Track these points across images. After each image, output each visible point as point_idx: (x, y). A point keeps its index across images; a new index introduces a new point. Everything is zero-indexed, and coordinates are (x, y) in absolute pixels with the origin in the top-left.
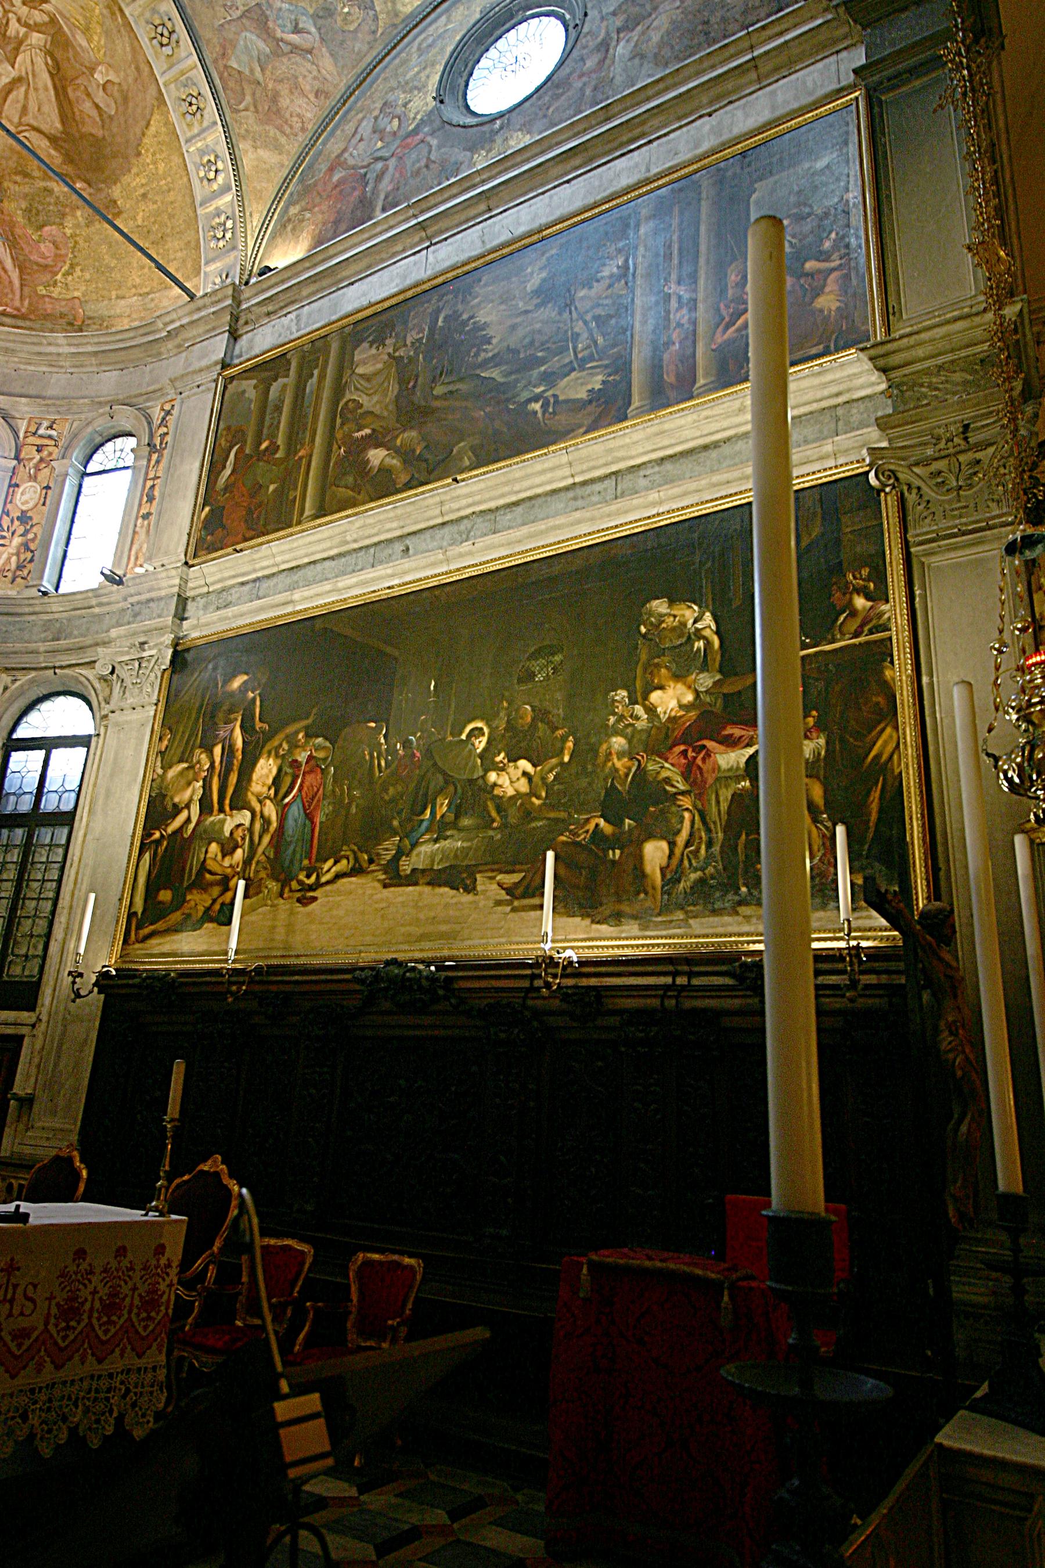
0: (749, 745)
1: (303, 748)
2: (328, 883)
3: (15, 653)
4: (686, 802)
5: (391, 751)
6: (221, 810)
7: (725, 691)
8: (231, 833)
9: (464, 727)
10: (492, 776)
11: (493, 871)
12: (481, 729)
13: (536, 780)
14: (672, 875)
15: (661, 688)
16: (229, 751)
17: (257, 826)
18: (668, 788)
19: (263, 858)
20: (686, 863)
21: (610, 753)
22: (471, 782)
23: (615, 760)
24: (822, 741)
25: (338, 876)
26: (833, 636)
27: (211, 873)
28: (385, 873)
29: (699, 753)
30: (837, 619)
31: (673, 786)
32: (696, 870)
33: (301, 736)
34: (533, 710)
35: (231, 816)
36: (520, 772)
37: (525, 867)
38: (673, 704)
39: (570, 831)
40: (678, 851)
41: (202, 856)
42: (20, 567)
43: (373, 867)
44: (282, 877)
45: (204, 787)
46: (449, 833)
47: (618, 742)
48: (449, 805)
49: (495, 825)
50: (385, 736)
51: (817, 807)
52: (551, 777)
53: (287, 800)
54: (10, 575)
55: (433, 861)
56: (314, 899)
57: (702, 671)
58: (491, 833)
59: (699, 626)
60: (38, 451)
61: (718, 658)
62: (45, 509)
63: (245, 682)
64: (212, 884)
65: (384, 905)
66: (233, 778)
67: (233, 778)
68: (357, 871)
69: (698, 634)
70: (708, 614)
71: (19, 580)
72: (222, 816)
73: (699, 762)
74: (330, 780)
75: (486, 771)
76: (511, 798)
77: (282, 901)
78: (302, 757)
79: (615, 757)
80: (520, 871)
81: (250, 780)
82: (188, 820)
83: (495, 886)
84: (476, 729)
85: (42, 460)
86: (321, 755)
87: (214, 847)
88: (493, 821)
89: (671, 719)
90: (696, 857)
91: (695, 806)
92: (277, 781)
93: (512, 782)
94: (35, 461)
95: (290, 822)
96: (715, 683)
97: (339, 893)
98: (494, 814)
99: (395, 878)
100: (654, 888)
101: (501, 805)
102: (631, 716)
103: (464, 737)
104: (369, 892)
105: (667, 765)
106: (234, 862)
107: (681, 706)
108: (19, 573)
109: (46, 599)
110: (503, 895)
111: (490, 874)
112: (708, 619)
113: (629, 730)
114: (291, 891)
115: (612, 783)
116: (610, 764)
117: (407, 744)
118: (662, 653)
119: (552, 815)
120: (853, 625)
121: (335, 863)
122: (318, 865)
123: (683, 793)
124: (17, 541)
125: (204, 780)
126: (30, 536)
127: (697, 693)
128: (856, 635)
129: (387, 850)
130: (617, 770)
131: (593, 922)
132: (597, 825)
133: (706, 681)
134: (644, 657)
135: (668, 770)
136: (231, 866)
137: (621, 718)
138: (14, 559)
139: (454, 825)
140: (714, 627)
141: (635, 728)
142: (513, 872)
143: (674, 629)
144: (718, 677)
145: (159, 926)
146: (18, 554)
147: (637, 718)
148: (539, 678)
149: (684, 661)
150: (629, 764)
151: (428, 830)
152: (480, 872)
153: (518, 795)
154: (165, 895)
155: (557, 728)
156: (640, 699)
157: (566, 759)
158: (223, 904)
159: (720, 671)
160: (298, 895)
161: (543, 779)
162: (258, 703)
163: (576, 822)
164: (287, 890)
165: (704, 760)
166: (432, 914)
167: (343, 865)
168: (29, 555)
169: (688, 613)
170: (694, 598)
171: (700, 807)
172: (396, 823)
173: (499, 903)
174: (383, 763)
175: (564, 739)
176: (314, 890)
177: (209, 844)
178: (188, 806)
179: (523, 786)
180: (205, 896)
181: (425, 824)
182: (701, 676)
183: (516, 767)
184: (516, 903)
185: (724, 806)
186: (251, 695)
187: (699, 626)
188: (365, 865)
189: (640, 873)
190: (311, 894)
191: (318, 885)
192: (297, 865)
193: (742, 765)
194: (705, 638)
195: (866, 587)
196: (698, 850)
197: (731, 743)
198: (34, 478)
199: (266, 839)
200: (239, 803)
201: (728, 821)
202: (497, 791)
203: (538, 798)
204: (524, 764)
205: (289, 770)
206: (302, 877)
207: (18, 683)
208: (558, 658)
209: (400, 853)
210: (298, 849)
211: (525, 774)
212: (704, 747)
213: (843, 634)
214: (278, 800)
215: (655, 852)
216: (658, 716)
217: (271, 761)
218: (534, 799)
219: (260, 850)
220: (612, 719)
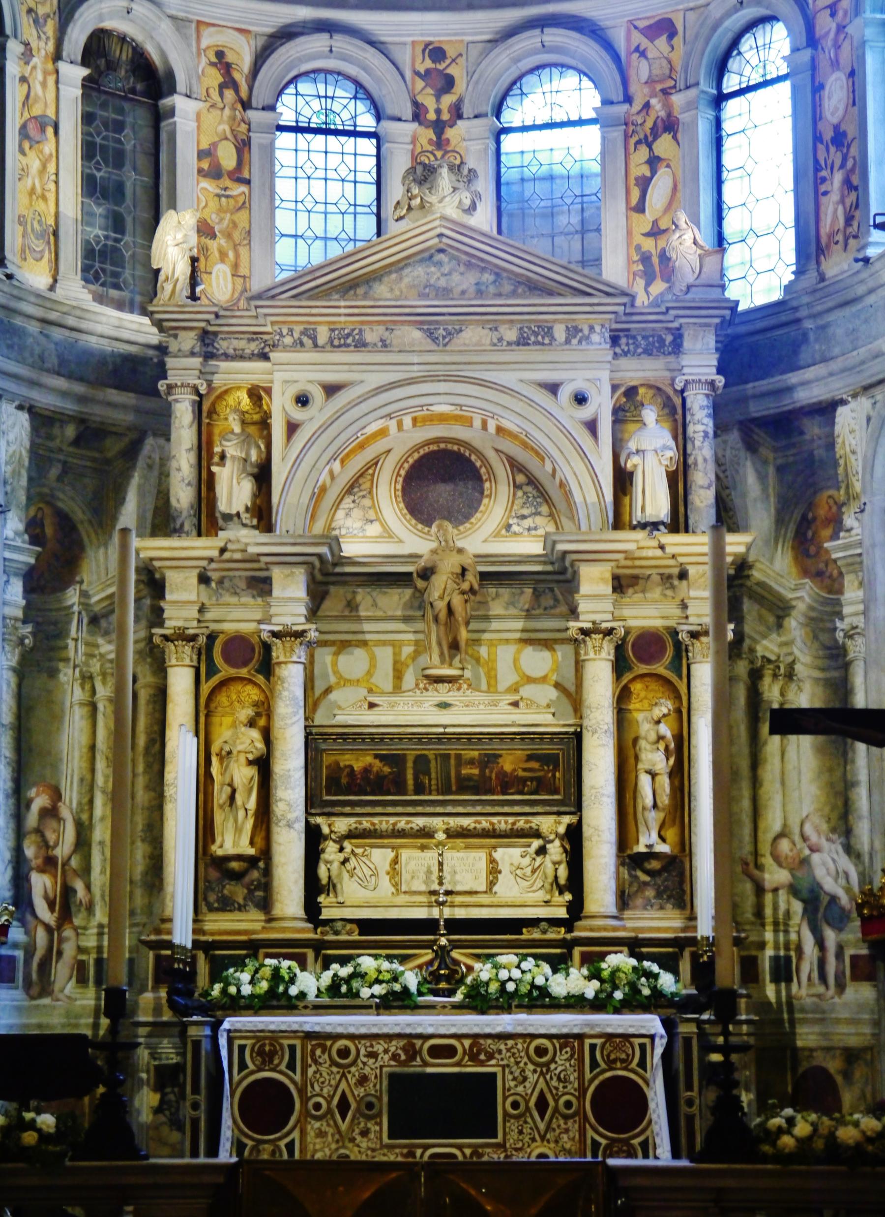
3: (863, 362)
42: (849, 220)
54: (840, 237)
60: (833, 15)
62: (856, 108)
71: (852, 242)
85: (841, 28)
94: (832, 35)
108: (850, 230)
109: (873, 269)
124: (838, 177)
126: (850, 164)
138: (840, 209)
146: (842, 201)
168: (853, 196)
198: (835, 64)
207: (878, 405)
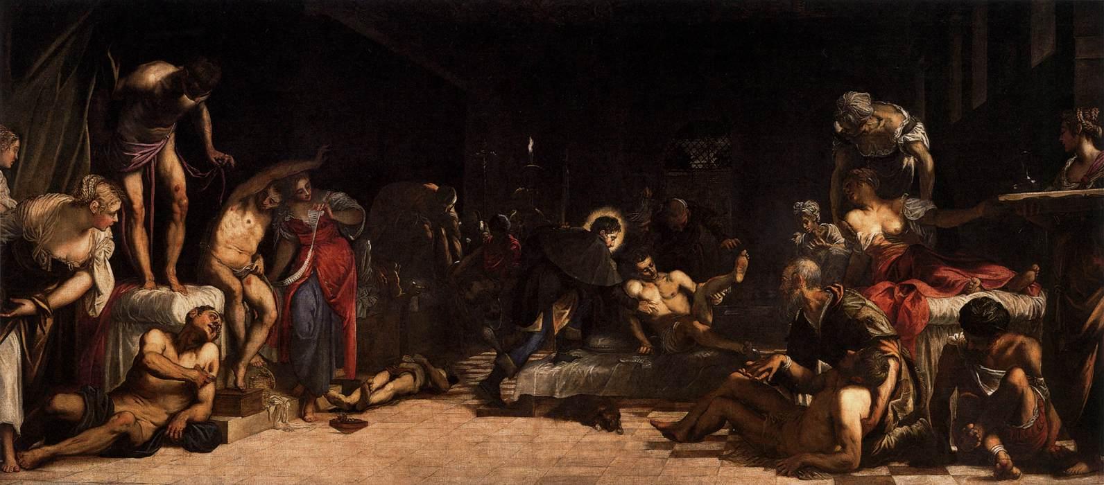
0: (965, 292)
1: (311, 203)
2: (382, 404)
4: (892, 348)
5: (469, 230)
6: (161, 280)
7: (939, 225)
8: (189, 318)
9: (588, 214)
10: (636, 287)
11: (644, 406)
12: (614, 221)
13: (699, 299)
14: (874, 429)
15: (863, 207)
16: (158, 187)
17: (240, 313)
18: (871, 330)
19: (258, 361)
20: (891, 415)
21: (798, 279)
22: (604, 291)
23: (805, 289)
24: (1042, 299)
25: (398, 397)
26: (1060, 182)
27: (156, 374)
28: (478, 397)
29: (908, 292)
30: (1064, 164)
31: (878, 329)
32: (901, 425)
33: (302, 184)
34: (689, 207)
35: (184, 292)
36: (674, 288)
37: (689, 405)
38: (876, 230)
39: (747, 367)
40: (882, 402)
41: (136, 349)
43: (455, 388)
44: (300, 389)
45: (117, 238)
46: (574, 354)
47: (809, 267)
48: (572, 318)
49: (643, 349)
50: (457, 207)
51: (1036, 370)
52: (719, 298)
53: (290, 280)
55: (553, 388)
56: (363, 424)
57: (913, 196)
58: (637, 360)
59: (910, 137)
61: (932, 182)
63: (171, 77)
64: (164, 392)
65: (481, 438)
66: (177, 235)
67: (177, 235)
68: (430, 390)
69: (908, 148)
70: (920, 125)
72: (164, 290)
73: (907, 304)
74: (367, 258)
75: (626, 278)
76: (664, 317)
77: (302, 423)
78: (311, 217)
79: (804, 284)
80: (681, 410)
81: (211, 239)
82: (93, 290)
83: (646, 425)
84: (607, 219)
86: (345, 219)
87: (156, 339)
88: (640, 344)
89: (876, 249)
90: (903, 410)
91: (902, 354)
92: (267, 248)
93: (664, 298)
95: (303, 314)
96: (926, 212)
97: (405, 419)
98: (640, 335)
99: (492, 403)
100: (854, 441)
101: (651, 323)
102: (824, 237)
103: (587, 227)
104: (454, 420)
105: (869, 303)
106: (201, 363)
107: (887, 235)
110: (659, 437)
111: (639, 410)
112: (919, 134)
113: (822, 253)
114: (318, 410)
115: (801, 314)
116: (798, 292)
117: (495, 223)
118: (864, 162)
119: (723, 345)
120: (1080, 173)
121: (392, 379)
122: (363, 378)
123: (888, 338)
125: (115, 228)
127: (906, 222)
128: (1083, 185)
129: (477, 366)
130: (807, 301)
131: (779, 473)
132: (782, 363)
133: (917, 208)
134: (840, 163)
135: (872, 308)
136: (196, 368)
137: (811, 237)
139: (583, 344)
140: (927, 144)
141: (829, 253)
142: (671, 409)
143: (878, 135)
144: (931, 207)
145: (65, 446)
147: (832, 240)
148: (697, 164)
149: (892, 184)
150: (823, 295)
151: (541, 347)
152: (624, 407)
153: (673, 316)
154: (69, 403)
155: (725, 237)
156: (835, 218)
157: (740, 278)
158: (190, 423)
159: (934, 199)
160: (333, 417)
161: (709, 300)
162: (206, 116)
163: (756, 357)
164: (310, 409)
165: (913, 302)
166: (557, 454)
167: (405, 382)
169: (897, 119)
170: (903, 100)
171: (908, 355)
172: (488, 332)
173: (653, 445)
174: (458, 246)
175: (736, 253)
176: (361, 412)
177: (148, 331)
178: (88, 265)
179: (680, 304)
180: (152, 409)
181: (535, 340)
182: (911, 201)
183: (670, 280)
184: (677, 447)
185: (935, 357)
186: (188, 102)
187: (910, 137)
188: (444, 384)
189: (835, 423)
190: (356, 417)
191: (365, 405)
192: (323, 378)
193: (956, 314)
194: (916, 155)
195: (1095, 132)
196: (905, 403)
197: (945, 288)
199: (260, 336)
200: (196, 270)
201: (938, 375)
202: (643, 307)
203: (703, 322)
204: (680, 277)
205: (287, 235)
206: (335, 392)
208: (721, 142)
209: (501, 372)
210: (325, 352)
211: (682, 289)
212: (913, 287)
213: (1069, 181)
214: (273, 277)
215: (854, 404)
216: (859, 242)
217: (249, 216)
218: (697, 324)
219: (252, 348)
220: (799, 237)
